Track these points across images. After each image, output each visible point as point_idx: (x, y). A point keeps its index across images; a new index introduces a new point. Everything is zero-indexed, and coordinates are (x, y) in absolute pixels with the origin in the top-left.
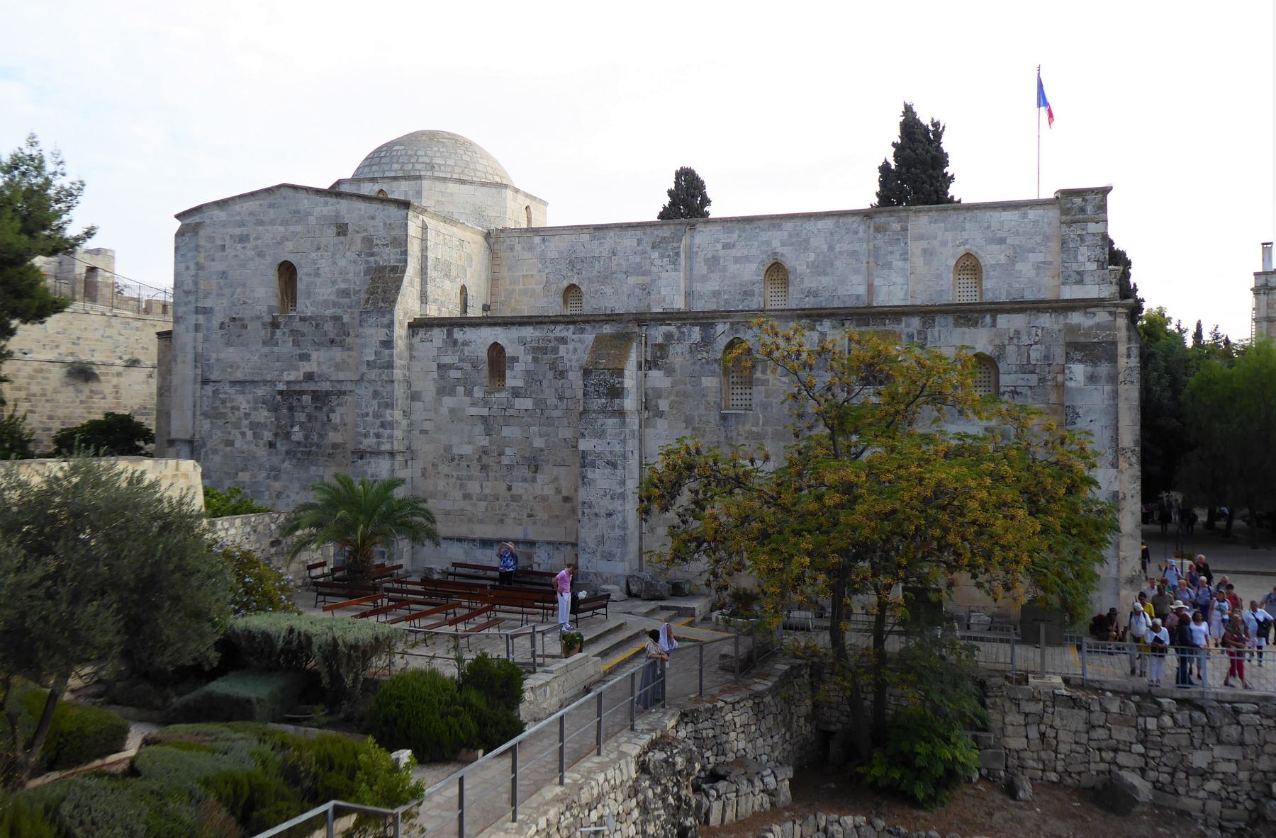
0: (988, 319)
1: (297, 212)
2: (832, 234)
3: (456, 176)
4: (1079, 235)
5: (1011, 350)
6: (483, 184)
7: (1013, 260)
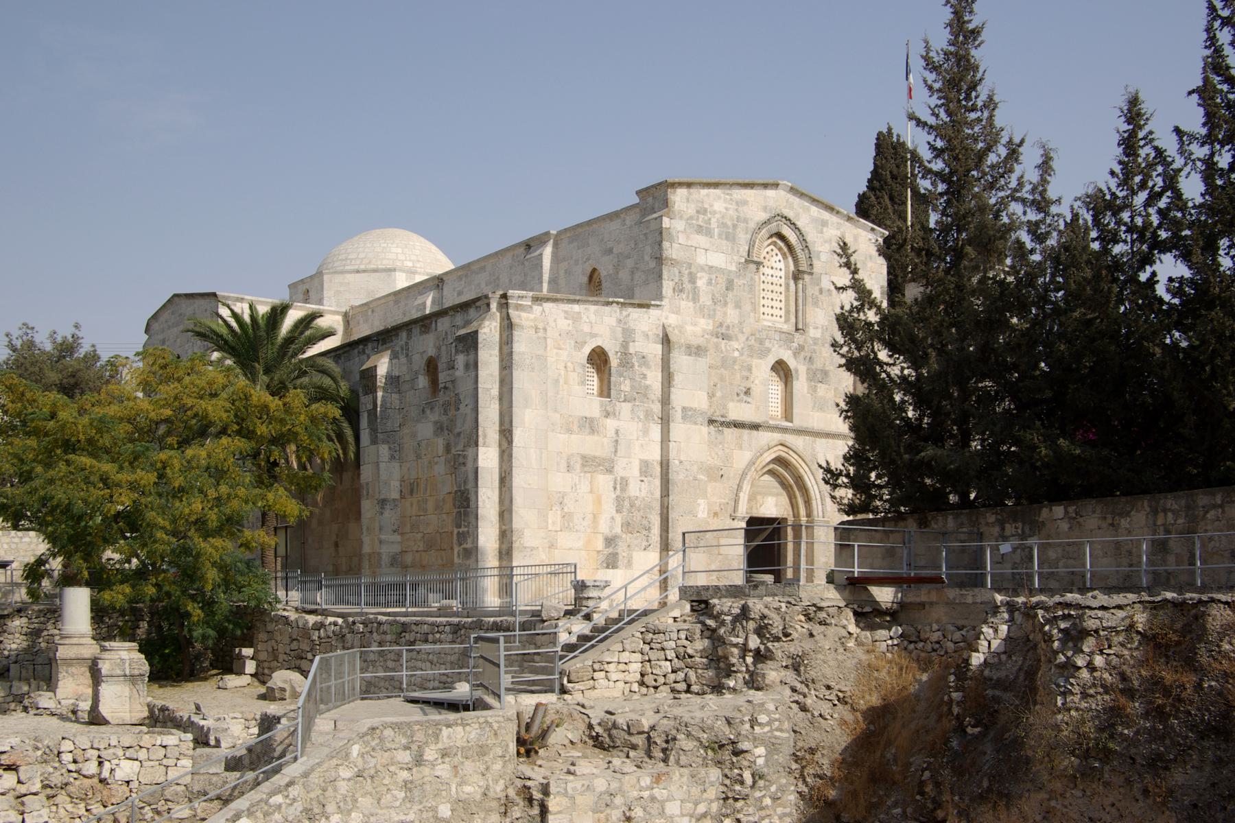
0: (433, 325)
1: (181, 315)
2: (511, 268)
3: (362, 267)
4: (645, 234)
5: (444, 348)
6: (375, 271)
7: (617, 268)
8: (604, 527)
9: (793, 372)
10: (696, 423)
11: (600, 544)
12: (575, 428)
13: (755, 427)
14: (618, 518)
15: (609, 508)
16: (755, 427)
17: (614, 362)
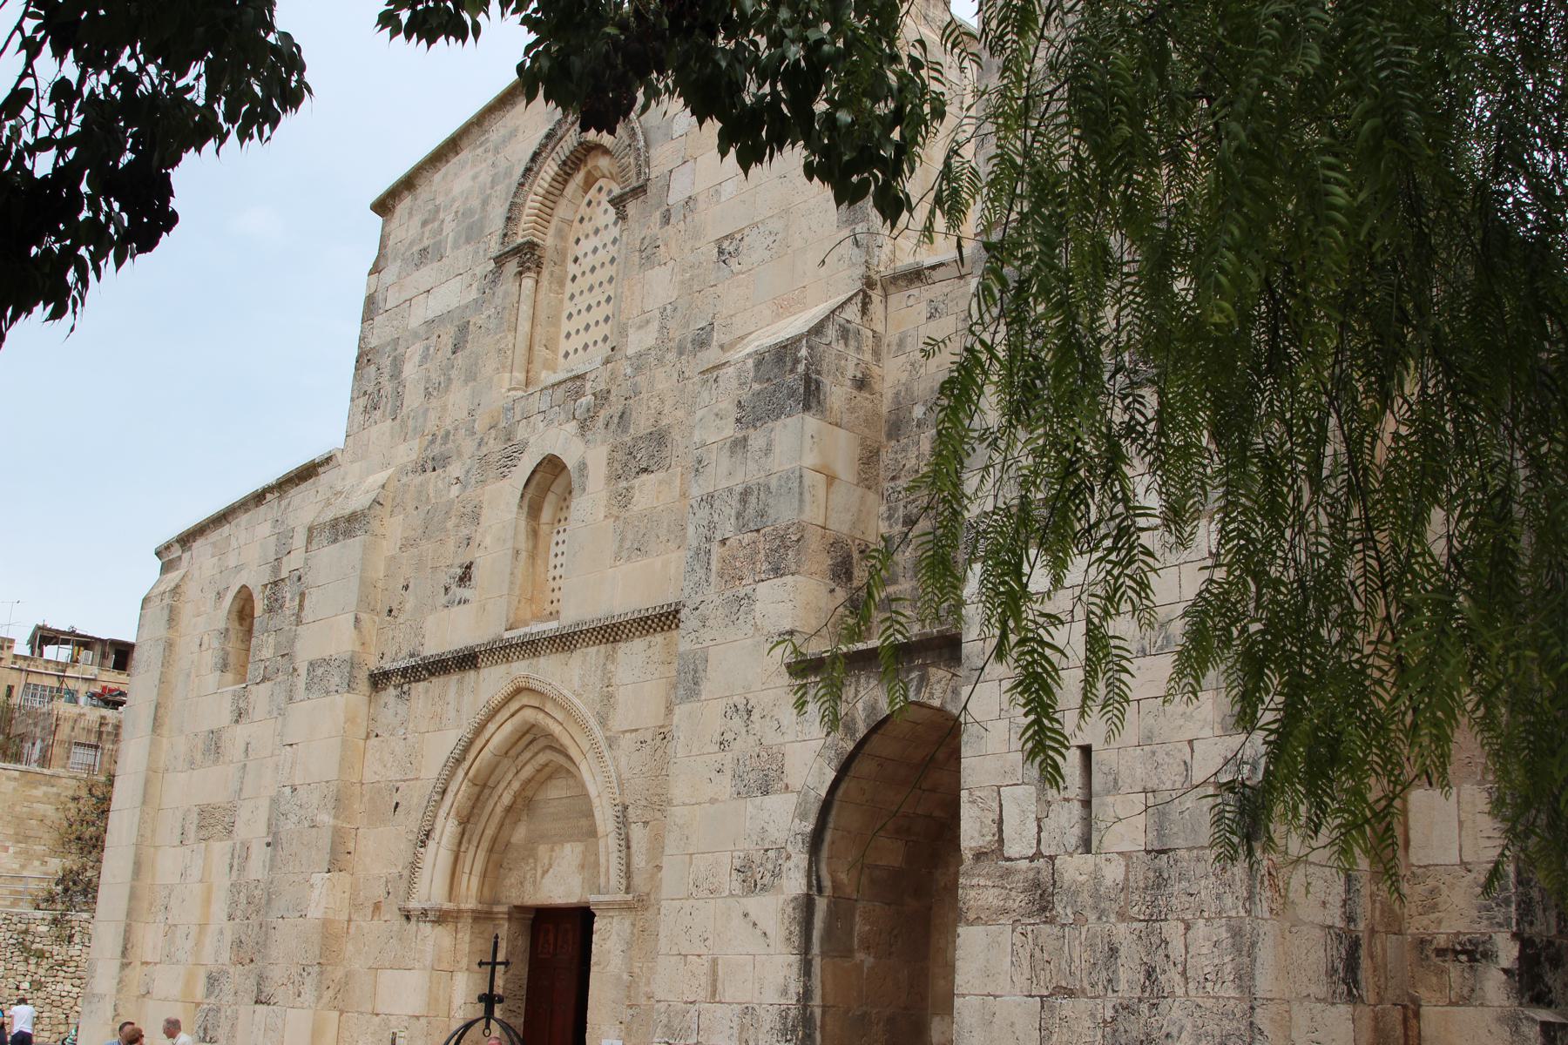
8: (208, 956)
9: (574, 476)
10: (327, 693)
11: (200, 991)
12: (198, 757)
13: (467, 660)
14: (228, 937)
15: (219, 909)
16: (467, 660)
17: (259, 606)
